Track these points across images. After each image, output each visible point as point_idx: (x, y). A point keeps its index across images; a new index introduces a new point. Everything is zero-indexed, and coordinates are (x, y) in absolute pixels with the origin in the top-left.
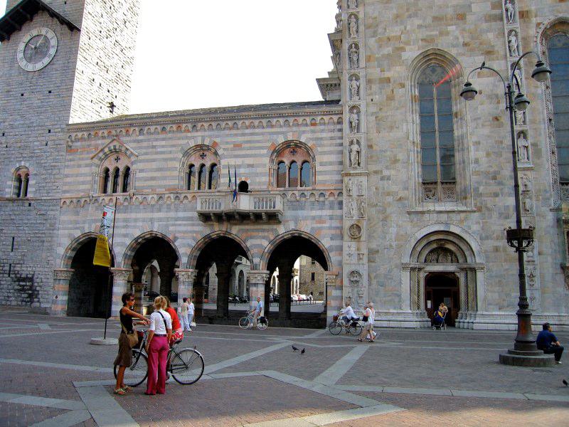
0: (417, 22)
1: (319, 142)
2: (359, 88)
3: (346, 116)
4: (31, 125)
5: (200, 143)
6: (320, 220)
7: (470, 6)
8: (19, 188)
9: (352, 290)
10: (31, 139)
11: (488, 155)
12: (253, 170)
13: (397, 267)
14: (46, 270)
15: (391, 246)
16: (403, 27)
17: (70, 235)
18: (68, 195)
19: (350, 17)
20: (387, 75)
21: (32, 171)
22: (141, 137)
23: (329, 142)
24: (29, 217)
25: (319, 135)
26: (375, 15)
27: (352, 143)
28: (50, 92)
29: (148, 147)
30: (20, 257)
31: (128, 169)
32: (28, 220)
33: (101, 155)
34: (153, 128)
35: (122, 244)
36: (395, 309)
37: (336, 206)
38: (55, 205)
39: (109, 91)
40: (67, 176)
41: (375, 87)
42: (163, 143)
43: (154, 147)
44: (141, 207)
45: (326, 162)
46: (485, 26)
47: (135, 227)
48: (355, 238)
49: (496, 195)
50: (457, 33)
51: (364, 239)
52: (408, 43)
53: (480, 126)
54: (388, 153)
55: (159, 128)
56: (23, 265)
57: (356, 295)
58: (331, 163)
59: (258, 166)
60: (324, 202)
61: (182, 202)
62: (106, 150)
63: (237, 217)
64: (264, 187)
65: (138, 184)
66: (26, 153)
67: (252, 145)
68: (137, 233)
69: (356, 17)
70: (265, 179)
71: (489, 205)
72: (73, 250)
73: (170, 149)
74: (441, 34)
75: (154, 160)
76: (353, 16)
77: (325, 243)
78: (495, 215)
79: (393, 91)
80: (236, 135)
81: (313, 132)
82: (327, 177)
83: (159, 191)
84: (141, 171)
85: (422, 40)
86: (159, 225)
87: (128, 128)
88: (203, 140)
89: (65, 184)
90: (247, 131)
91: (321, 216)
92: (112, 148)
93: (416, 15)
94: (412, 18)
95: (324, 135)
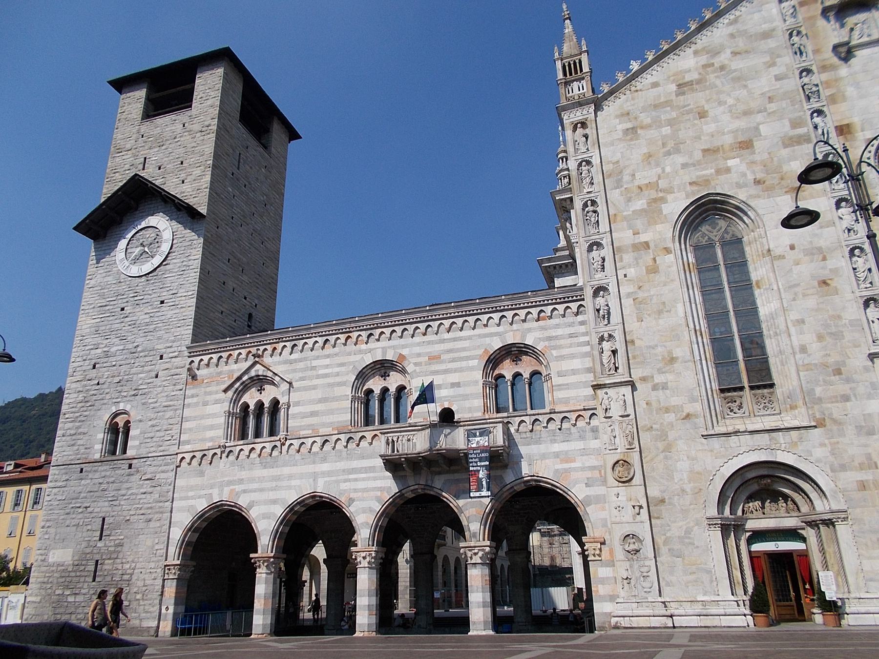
0: (680, 159)
1: (553, 343)
2: (604, 259)
3: (588, 302)
4: (134, 350)
6: (566, 457)
7: (757, 128)
8: (114, 443)
9: (631, 566)
10: (134, 370)
11: (820, 338)
12: (460, 391)
13: (697, 523)
14: (152, 565)
15: (683, 490)
16: (659, 170)
17: (189, 509)
18: (188, 448)
19: (580, 165)
20: (643, 238)
21: (135, 416)
22: (295, 356)
23: (569, 341)
25: (553, 333)
26: (615, 159)
27: (602, 339)
28: (162, 302)
31: (275, 403)
34: (311, 342)
35: (266, 516)
36: (705, 595)
37: (589, 434)
38: (167, 464)
39: (245, 298)
41: (628, 258)
42: (327, 361)
43: (313, 368)
44: (298, 456)
45: (567, 371)
46: (785, 152)
47: (289, 488)
48: (624, 482)
49: (846, 398)
50: (743, 168)
51: (638, 483)
52: (669, 191)
53: (801, 296)
54: (659, 349)
56: (118, 561)
57: (638, 574)
58: (574, 372)
59: (468, 384)
60: (570, 429)
61: (358, 445)
62: (245, 378)
63: (441, 461)
64: (479, 414)
66: (127, 390)
67: (456, 355)
68: (292, 497)
69: (588, 163)
70: (479, 403)
71: (835, 416)
72: (194, 531)
74: (718, 172)
75: (314, 388)
76: (584, 163)
77: (577, 493)
78: (850, 430)
79: (654, 259)
81: (543, 328)
82: (572, 393)
83: (322, 431)
84: (297, 404)
85: (690, 183)
86: (326, 482)
87: (274, 345)
91: (567, 452)
93: (677, 151)
94: (672, 157)
95: (559, 332)
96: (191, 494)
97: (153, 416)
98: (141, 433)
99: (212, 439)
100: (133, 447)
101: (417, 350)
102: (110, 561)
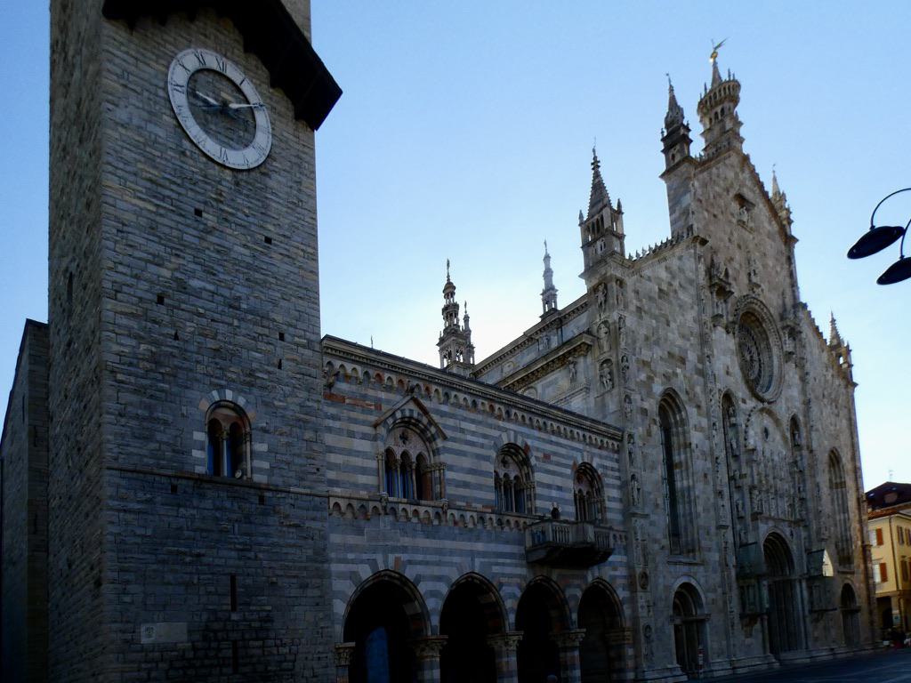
5: (512, 441)
17: (353, 576)
18: (338, 490)
20: (646, 405)
22: (444, 408)
24: (264, 529)
29: (455, 429)
30: (256, 625)
32: (266, 535)
33: (390, 421)
34: (461, 396)
40: (330, 450)
42: (473, 427)
43: (462, 431)
55: (470, 400)
56: (270, 642)
65: (450, 490)
73: (481, 440)
80: (544, 440)
84: (451, 468)
88: (516, 437)
89: (331, 466)
90: (554, 438)
92: (407, 414)
96: (351, 556)
97: (286, 429)
98: (269, 451)
99: (365, 487)
100: (261, 471)
101: (537, 444)
102: (259, 643)
